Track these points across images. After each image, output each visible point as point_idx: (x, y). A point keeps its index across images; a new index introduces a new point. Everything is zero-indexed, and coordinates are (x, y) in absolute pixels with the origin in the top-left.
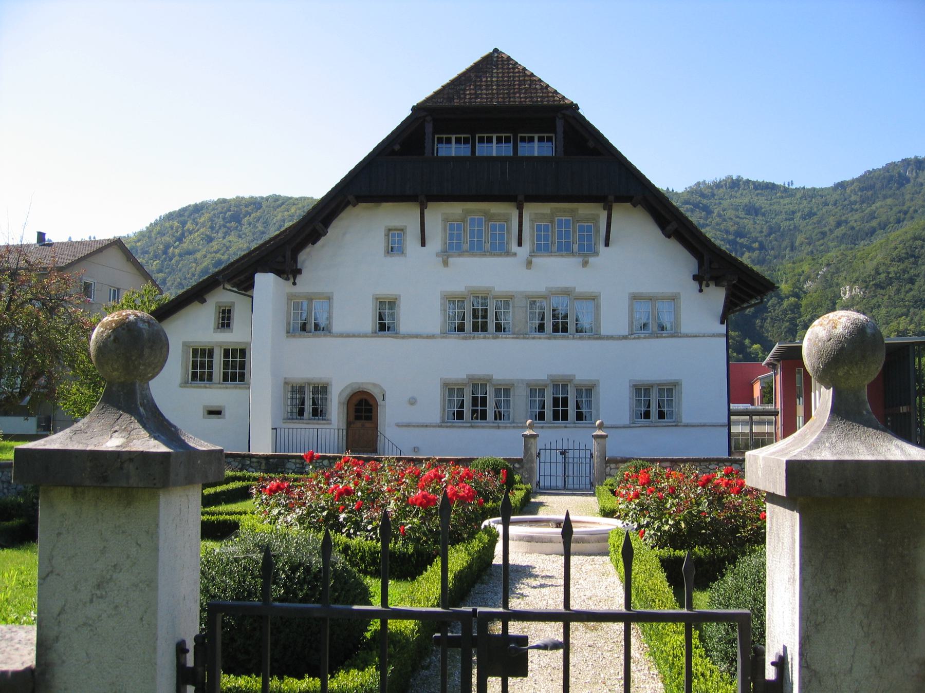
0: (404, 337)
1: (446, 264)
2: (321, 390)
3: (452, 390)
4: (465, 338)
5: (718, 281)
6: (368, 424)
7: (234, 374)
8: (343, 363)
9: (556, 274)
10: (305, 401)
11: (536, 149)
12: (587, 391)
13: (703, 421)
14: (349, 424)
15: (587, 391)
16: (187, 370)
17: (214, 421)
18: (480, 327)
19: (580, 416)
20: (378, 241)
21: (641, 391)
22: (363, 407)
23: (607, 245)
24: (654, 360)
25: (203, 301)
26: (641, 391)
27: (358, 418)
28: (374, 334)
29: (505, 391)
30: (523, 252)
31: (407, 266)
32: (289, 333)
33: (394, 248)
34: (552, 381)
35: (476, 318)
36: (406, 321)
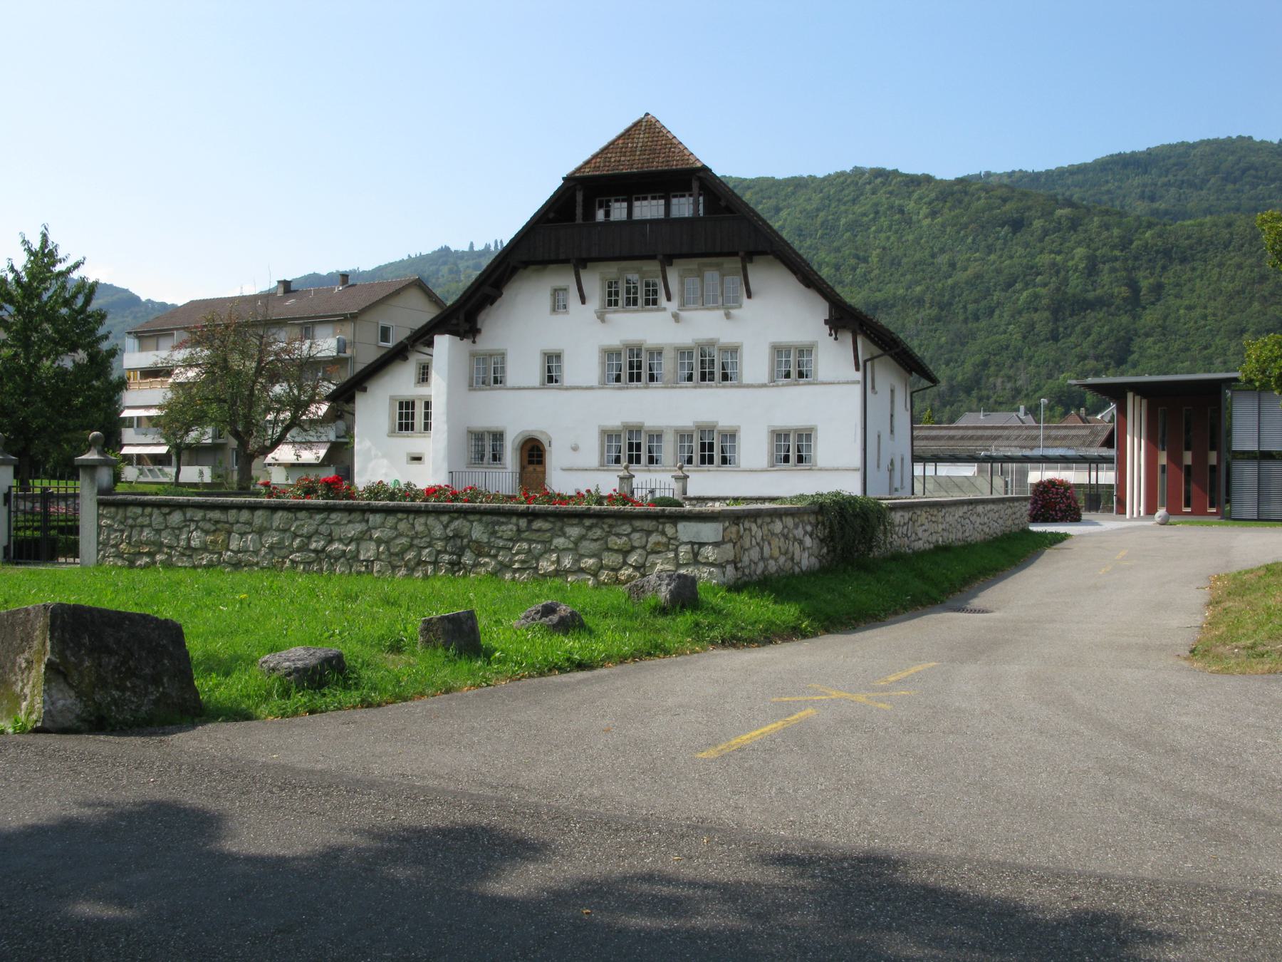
0: (567, 389)
1: (603, 321)
2: (498, 437)
3: (609, 436)
4: (620, 388)
5: (844, 327)
6: (539, 468)
7: (407, 425)
8: (518, 412)
9: (705, 326)
10: (484, 445)
11: (683, 207)
12: (731, 436)
13: (836, 466)
14: (523, 468)
15: (731, 436)
16: (394, 421)
17: (416, 465)
18: (635, 378)
19: (724, 461)
20: (545, 299)
21: (780, 436)
22: (533, 452)
23: (749, 296)
24: (792, 406)
25: (405, 359)
26: (780, 436)
27: (531, 462)
28: (542, 387)
29: (656, 436)
30: (673, 306)
31: (560, 325)
32: (471, 387)
33: (558, 305)
34: (698, 427)
35: (632, 367)
36: (571, 372)
